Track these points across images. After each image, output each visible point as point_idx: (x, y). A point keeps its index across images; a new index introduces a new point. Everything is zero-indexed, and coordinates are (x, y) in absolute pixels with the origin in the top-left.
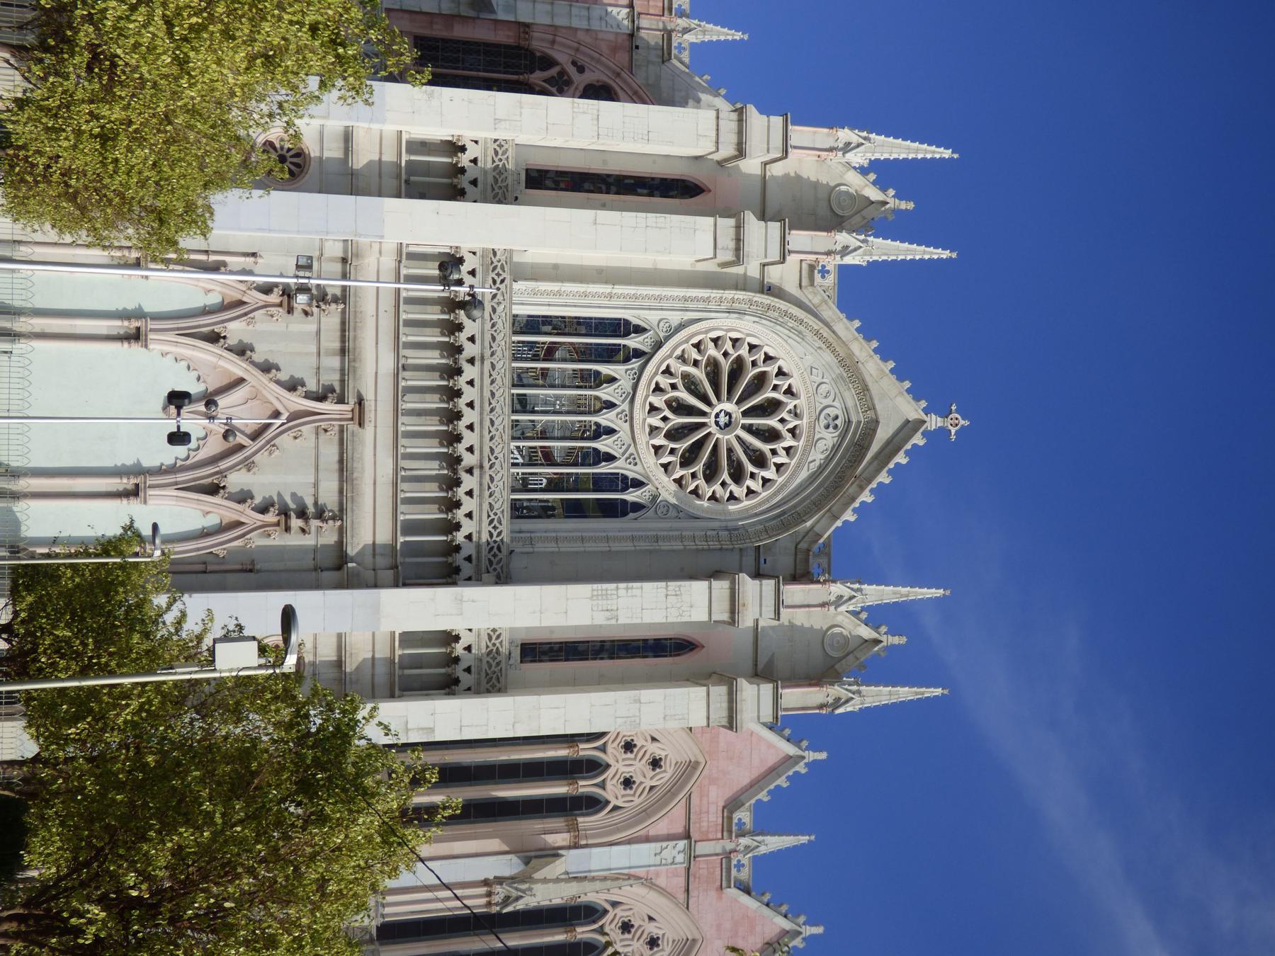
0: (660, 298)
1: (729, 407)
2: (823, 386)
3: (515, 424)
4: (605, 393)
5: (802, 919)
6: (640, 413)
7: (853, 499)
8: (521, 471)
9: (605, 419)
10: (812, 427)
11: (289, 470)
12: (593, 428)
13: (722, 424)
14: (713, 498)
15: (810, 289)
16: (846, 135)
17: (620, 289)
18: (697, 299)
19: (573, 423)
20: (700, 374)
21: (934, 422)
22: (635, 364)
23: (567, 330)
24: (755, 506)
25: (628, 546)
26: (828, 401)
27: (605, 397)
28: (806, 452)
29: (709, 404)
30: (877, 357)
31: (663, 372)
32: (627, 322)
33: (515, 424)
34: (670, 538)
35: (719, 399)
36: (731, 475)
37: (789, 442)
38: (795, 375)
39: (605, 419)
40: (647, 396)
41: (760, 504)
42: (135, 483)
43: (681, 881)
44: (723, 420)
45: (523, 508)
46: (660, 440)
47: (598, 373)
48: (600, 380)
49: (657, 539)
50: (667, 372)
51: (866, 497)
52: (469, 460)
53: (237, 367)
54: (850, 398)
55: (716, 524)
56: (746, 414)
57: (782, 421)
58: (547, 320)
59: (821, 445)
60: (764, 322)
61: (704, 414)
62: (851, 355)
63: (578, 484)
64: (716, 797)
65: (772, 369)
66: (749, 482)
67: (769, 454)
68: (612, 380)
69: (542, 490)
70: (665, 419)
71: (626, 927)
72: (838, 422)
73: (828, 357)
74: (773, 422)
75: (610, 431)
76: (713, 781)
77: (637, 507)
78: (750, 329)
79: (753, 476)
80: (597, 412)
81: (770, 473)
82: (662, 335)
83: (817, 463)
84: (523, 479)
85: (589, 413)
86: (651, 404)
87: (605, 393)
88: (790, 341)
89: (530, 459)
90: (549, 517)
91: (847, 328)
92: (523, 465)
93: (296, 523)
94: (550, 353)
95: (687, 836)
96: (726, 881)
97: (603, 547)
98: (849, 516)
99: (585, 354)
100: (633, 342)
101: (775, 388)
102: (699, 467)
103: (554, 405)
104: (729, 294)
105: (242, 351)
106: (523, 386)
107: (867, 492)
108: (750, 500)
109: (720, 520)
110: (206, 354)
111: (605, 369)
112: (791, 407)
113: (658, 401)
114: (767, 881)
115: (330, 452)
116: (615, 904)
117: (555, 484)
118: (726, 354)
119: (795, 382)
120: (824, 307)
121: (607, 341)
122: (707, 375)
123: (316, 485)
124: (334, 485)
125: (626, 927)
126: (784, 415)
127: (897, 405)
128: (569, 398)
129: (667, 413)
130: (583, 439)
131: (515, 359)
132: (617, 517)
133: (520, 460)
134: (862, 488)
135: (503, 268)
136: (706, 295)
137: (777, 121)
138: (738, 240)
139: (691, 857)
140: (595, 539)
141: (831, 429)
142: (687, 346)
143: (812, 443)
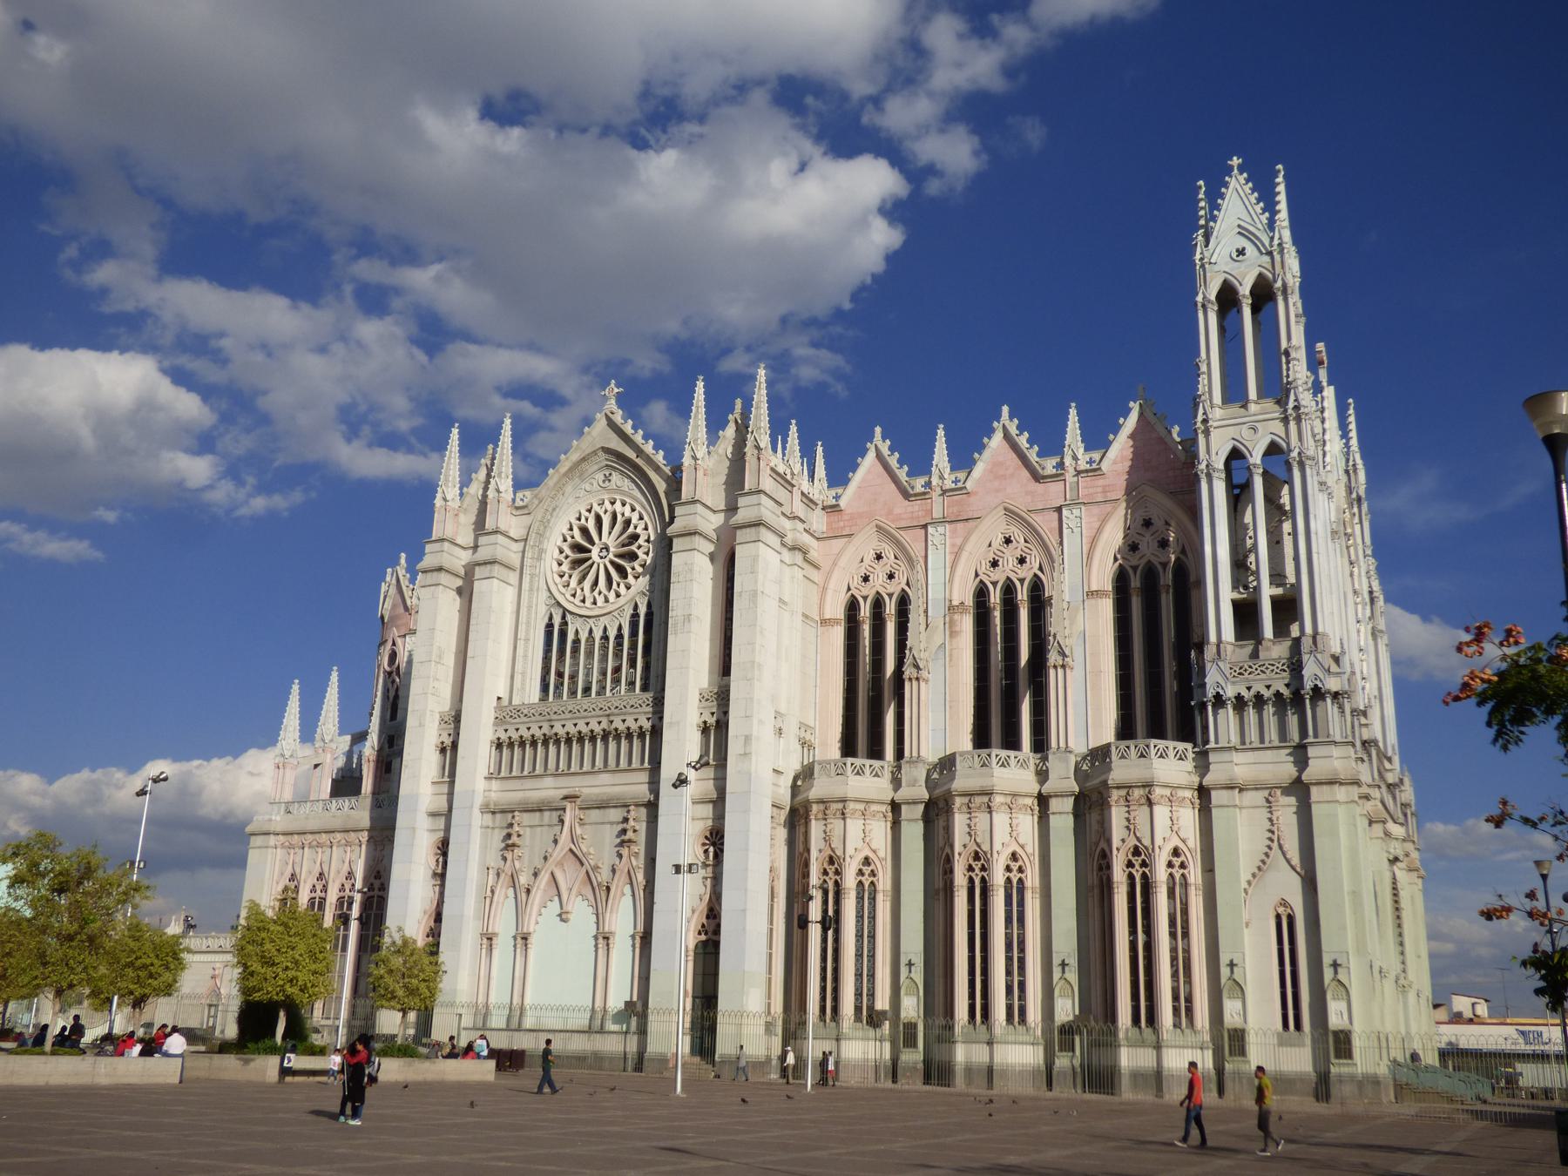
0: (530, 607)
4: (583, 636)
5: (995, 424)
9: (598, 634)
11: (599, 841)
14: (647, 554)
16: (438, 502)
17: (521, 635)
20: (576, 575)
21: (612, 404)
22: (569, 617)
28: (623, 493)
33: (598, 694)
43: (960, 525)
44: (604, 553)
48: (577, 642)
51: (649, 448)
52: (604, 725)
53: (545, 877)
62: (565, 474)
63: (633, 646)
64: (901, 506)
71: (995, 564)
73: (569, 489)
75: (605, 629)
76: (890, 512)
77: (649, 605)
87: (583, 636)
93: (630, 834)
94: (560, 675)
95: (925, 527)
96: (959, 490)
98: (659, 457)
100: (557, 621)
104: (528, 562)
105: (536, 875)
108: (646, 529)
110: (537, 896)
114: (962, 459)
115: (595, 815)
116: (977, 575)
117: (633, 663)
121: (556, 637)
123: (612, 823)
124: (612, 811)
125: (995, 564)
127: (599, 434)
135: (506, 713)
137: (428, 548)
138: (485, 563)
139: (943, 521)
143: (618, 490)
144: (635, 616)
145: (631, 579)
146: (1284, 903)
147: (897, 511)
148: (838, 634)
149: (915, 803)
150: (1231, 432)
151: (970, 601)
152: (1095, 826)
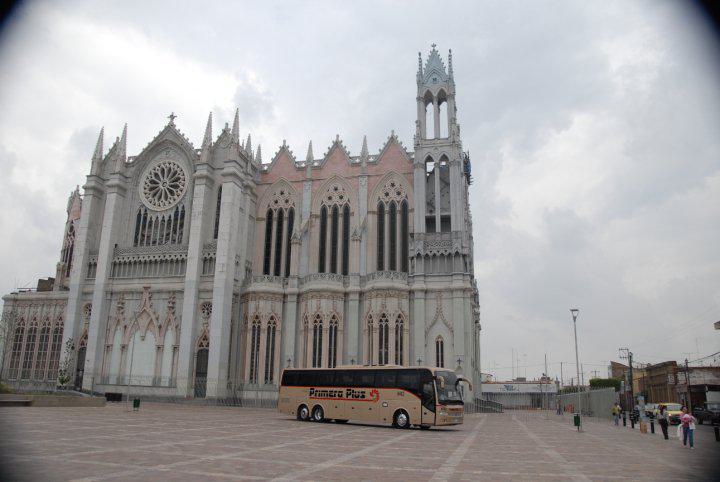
1: (161, 187)
4: (154, 220)
9: (160, 219)
22: (148, 212)
42: (159, 348)
48: (151, 222)
58: (136, 237)
63: (175, 225)
87: (154, 220)
94: (143, 236)
100: (143, 212)
115: (156, 296)
121: (142, 220)
144: (177, 212)
146: (440, 337)
147: (291, 174)
148: (263, 225)
149: (294, 294)
150: (428, 150)
151: (319, 213)
152: (368, 305)
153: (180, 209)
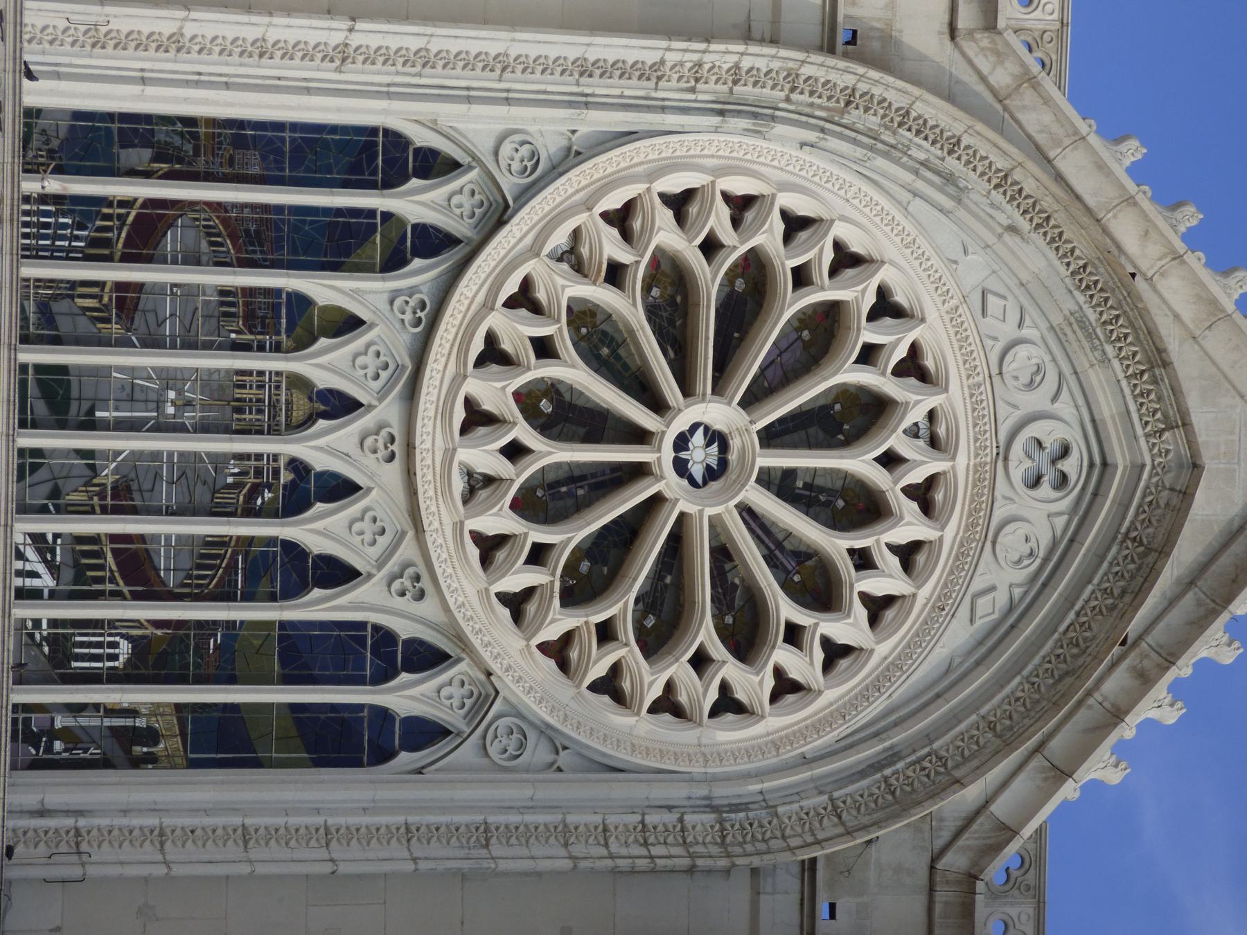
0: (502, 65)
2: (1022, 351)
3: (29, 463)
4: (324, 365)
6: (433, 432)
7: (1117, 715)
8: (47, 612)
9: (324, 448)
10: (985, 483)
12: (285, 477)
13: (697, 471)
14: (668, 704)
15: (984, 40)
18: (622, 70)
19: (219, 460)
20: (626, 308)
22: (421, 274)
23: (200, 165)
24: (802, 734)
25: (395, 858)
26: (1037, 400)
27: (323, 379)
28: (965, 560)
29: (658, 405)
30: (1196, 261)
31: (511, 303)
32: (396, 140)
33: (29, 463)
34: (526, 834)
35: (687, 390)
36: (725, 634)
37: (909, 526)
38: (932, 315)
39: (324, 448)
40: (460, 378)
41: (818, 727)
44: (700, 455)
45: (53, 734)
46: (497, 519)
47: (301, 302)
48: (304, 324)
49: (485, 834)
50: (524, 299)
51: (1159, 708)
54: (1109, 391)
55: (676, 793)
56: (771, 437)
57: (890, 460)
59: (1012, 540)
60: (833, 143)
61: (640, 436)
62: (1111, 251)
65: (857, 294)
66: (783, 655)
67: (845, 566)
68: (347, 324)
69: (115, 678)
70: (515, 451)
72: (1070, 466)
73: (1036, 258)
74: (858, 463)
75: (339, 489)
77: (423, 733)
78: (787, 166)
79: (794, 635)
80: (298, 426)
81: (847, 627)
82: (509, 184)
83: (1001, 598)
84: (53, 640)
85: (273, 430)
86: (469, 403)
87: (324, 365)
88: (917, 205)
89: (79, 578)
90: (137, 763)
91: (1101, 167)
92: (53, 595)
94: (146, 233)
97: (312, 861)
99: (257, 238)
100: (415, 203)
101: (869, 354)
102: (621, 606)
103: (159, 404)
104: (723, 55)
106: (56, 341)
107: (1161, 690)
109: (690, 779)
111: (325, 289)
112: (916, 415)
113: (494, 391)
117: (159, 658)
118: (710, 247)
119: (933, 333)
120: (1028, 96)
121: (332, 197)
122: (652, 312)
126: (896, 441)
128: (206, 380)
129: (523, 432)
130: (250, 512)
131: (31, 254)
132: (358, 763)
133: (46, 581)
134: (1145, 680)
136: (651, 57)
140: (285, 836)
141: (1045, 490)
142: (589, 220)
143: (984, 533)
145: (558, 622)
153: (406, 696)
